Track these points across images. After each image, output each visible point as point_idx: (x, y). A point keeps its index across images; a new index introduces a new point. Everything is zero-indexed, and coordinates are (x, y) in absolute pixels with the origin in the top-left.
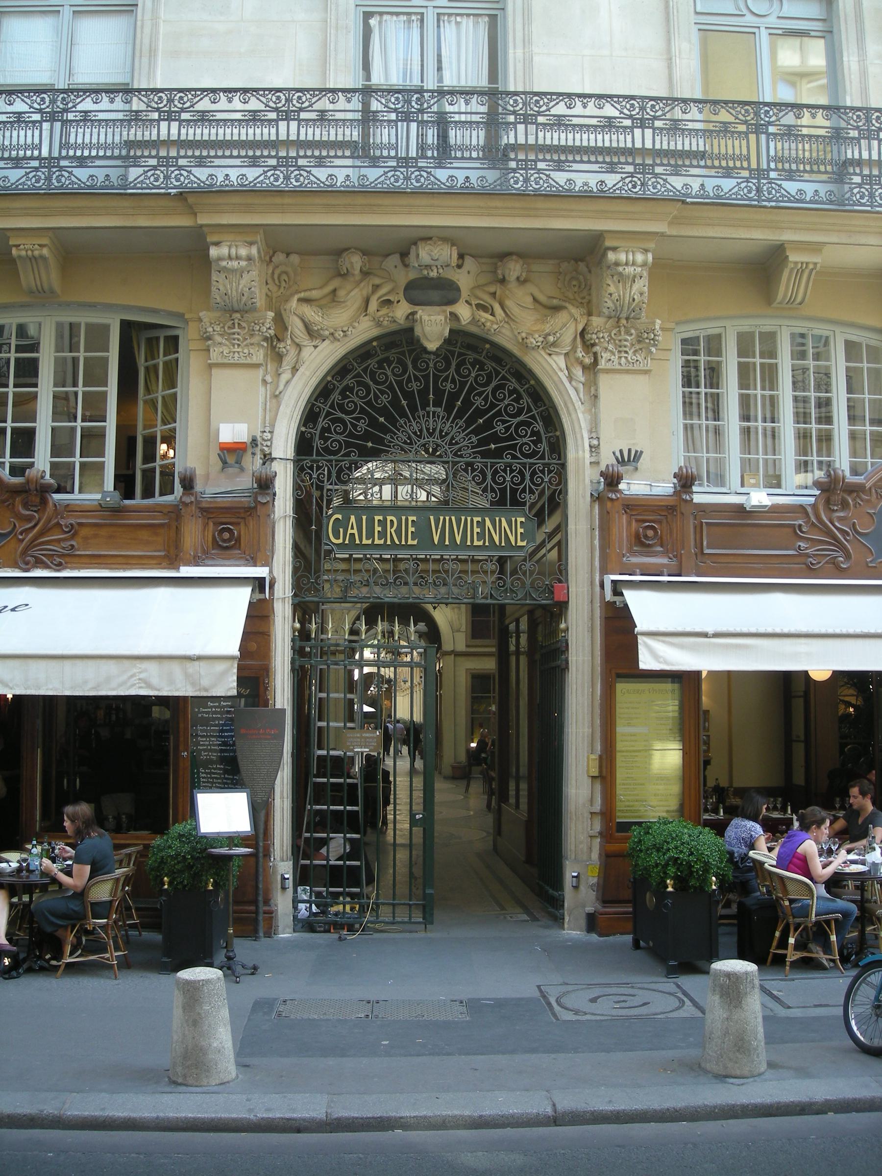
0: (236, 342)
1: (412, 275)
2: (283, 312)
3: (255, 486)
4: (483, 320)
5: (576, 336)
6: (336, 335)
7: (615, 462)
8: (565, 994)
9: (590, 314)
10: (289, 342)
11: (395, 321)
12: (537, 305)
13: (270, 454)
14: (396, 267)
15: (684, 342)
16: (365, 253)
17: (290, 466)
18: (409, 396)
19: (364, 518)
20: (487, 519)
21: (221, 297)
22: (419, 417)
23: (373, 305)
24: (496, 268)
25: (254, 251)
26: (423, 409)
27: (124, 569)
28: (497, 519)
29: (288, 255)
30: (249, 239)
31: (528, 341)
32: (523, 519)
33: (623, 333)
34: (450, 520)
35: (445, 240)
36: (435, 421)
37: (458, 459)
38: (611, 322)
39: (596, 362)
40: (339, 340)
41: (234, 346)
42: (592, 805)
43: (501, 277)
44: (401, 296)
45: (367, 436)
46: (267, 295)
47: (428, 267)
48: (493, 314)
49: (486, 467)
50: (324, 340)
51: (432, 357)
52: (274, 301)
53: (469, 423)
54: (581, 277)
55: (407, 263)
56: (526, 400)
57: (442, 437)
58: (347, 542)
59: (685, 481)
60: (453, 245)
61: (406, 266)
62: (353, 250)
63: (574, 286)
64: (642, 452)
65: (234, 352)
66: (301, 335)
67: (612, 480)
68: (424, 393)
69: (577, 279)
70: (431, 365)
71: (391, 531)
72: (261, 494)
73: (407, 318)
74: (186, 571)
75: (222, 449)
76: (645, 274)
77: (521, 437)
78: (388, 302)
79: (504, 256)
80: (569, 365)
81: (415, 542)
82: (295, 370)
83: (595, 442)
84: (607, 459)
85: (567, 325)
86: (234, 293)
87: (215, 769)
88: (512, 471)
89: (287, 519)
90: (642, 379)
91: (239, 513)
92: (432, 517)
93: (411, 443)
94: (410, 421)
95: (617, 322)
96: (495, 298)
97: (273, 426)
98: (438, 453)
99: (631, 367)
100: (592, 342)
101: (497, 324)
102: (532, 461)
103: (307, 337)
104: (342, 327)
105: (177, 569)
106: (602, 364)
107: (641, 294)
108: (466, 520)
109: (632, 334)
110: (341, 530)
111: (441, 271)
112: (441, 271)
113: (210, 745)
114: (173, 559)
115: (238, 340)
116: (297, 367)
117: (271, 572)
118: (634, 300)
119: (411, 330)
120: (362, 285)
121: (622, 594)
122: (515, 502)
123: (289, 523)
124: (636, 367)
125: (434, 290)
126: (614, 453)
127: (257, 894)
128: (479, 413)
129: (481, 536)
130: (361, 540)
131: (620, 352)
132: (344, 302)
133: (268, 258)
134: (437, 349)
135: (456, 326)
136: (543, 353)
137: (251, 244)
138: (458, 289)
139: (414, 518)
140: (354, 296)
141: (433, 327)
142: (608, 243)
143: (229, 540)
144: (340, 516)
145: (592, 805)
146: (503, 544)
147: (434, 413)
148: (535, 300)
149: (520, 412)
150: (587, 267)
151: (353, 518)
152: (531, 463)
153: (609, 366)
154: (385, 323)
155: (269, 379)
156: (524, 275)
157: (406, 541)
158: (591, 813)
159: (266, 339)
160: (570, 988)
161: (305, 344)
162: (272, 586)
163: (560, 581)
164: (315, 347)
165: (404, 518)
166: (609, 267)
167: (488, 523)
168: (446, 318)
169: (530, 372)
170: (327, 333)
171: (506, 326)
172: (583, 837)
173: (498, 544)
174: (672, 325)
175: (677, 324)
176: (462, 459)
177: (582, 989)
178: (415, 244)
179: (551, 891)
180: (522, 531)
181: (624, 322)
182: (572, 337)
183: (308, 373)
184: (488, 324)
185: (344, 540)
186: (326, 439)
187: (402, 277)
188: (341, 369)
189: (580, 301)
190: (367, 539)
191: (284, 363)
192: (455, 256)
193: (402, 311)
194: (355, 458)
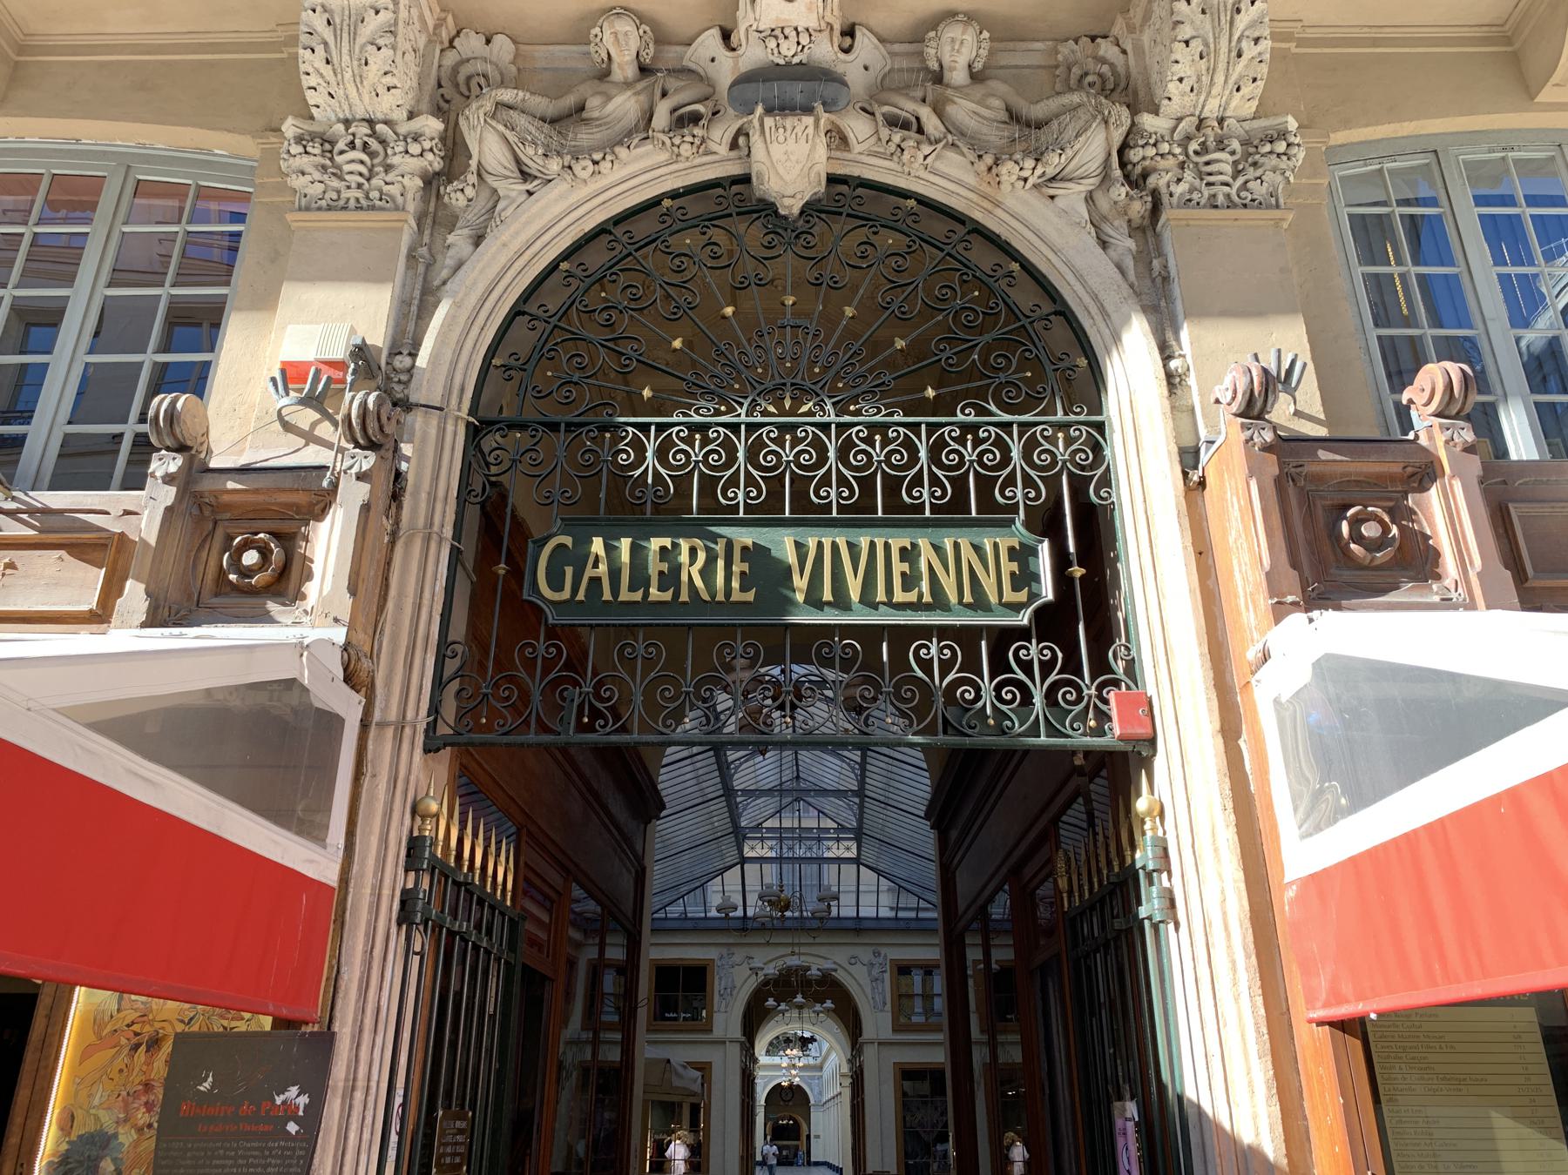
6: (577, 168)
10: (472, 178)
14: (713, 60)
20: (924, 544)
29: (488, 41)
34: (835, 546)
37: (847, 419)
55: (734, 45)
58: (581, 596)
73: (734, 145)
78: (695, 118)
81: (750, 596)
86: (346, 58)
98: (804, 409)
102: (1026, 418)
108: (872, 545)
110: (569, 571)
111: (804, 40)
112: (804, 40)
115: (361, 174)
119: (745, 179)
120: (640, 86)
125: (792, 87)
129: (909, 582)
130: (615, 590)
141: (790, 162)
144: (568, 540)
148: (1008, 110)
151: (597, 546)
152: (1021, 424)
156: (983, 53)
164: (530, 193)
176: (860, 419)
187: (725, 69)
190: (632, 589)
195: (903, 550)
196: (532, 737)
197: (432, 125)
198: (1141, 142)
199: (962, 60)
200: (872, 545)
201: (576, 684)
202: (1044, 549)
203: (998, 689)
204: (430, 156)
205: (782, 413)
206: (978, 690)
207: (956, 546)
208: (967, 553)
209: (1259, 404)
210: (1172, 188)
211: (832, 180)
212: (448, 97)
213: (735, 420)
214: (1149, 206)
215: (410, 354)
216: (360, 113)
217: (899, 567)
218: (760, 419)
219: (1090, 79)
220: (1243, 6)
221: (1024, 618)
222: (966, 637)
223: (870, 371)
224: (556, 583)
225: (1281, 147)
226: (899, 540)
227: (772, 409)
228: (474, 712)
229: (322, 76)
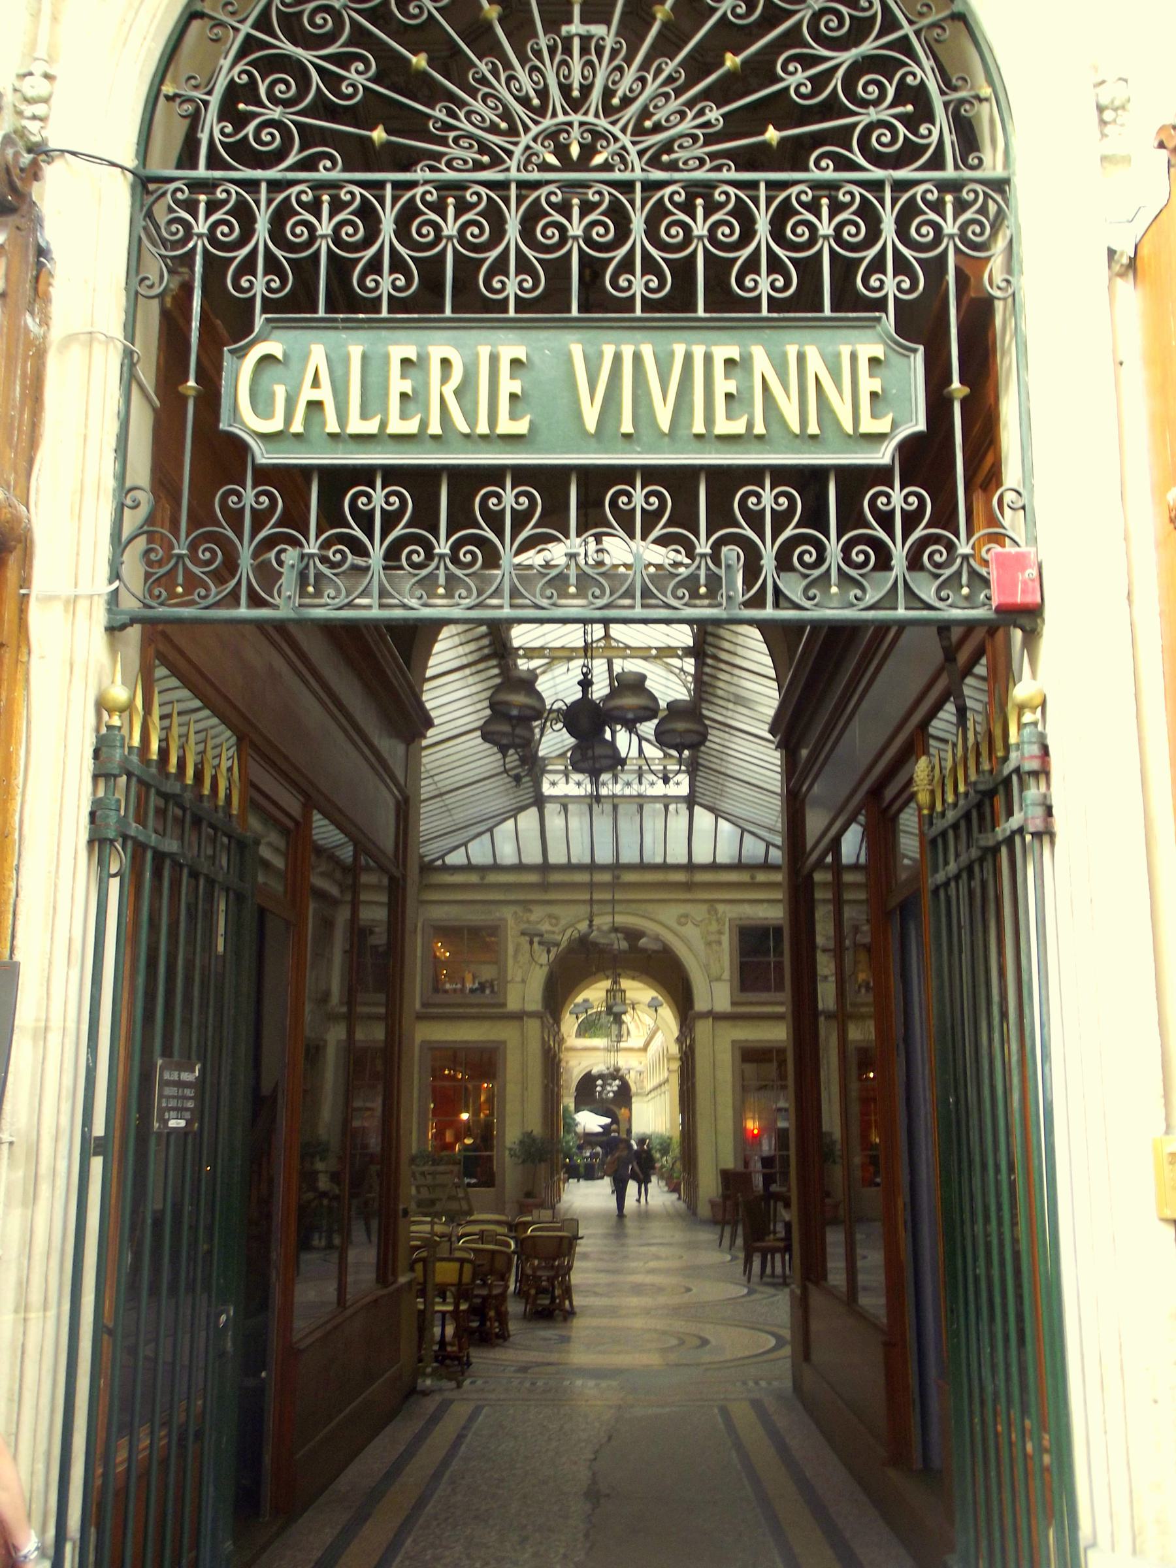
20: (759, 354)
26: (552, 26)
28: (792, 351)
32: (878, 351)
34: (637, 358)
37: (657, 175)
57: (608, 110)
77: (864, 104)
81: (521, 427)
92: (577, 350)
94: (508, 66)
98: (598, 160)
108: (688, 358)
110: (280, 391)
122: (847, 299)
130: (342, 419)
139: (520, 353)
144: (273, 346)
147: (585, 39)
151: (318, 355)
165: (484, 352)
167: (761, 363)
173: (796, 429)
176: (677, 176)
190: (364, 416)
194: (335, 175)
195: (729, 362)
196: (244, 611)
200: (688, 358)
201: (295, 543)
202: (918, 360)
203: (846, 550)
205: (567, 164)
206: (821, 549)
207: (801, 358)
208: (815, 365)
213: (500, 177)
215: (47, 76)
218: (536, 176)
221: (883, 455)
222: (809, 480)
223: (690, 104)
226: (725, 350)
227: (552, 160)
228: (168, 580)
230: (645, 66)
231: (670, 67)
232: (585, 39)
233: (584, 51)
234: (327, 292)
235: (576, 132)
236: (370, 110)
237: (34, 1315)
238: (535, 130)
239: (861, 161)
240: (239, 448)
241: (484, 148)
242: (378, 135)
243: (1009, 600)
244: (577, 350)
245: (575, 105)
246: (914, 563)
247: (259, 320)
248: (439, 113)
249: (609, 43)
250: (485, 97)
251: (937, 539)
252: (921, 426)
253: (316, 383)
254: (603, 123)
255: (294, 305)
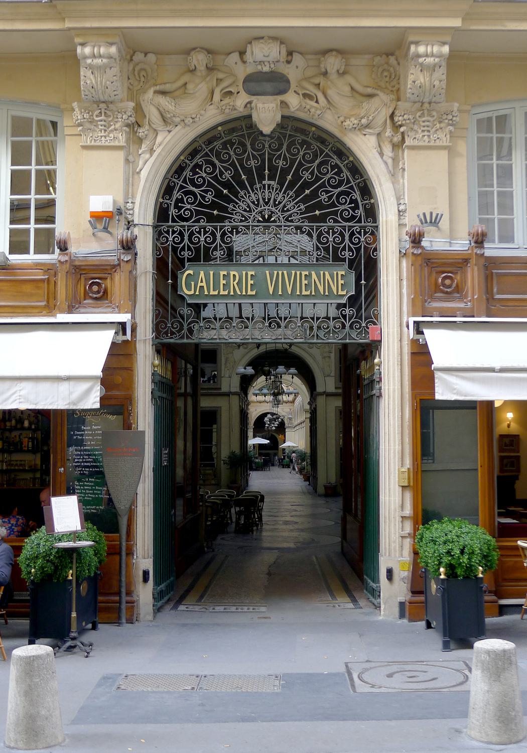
0: (103, 127)
1: (250, 69)
2: (142, 102)
3: (119, 246)
4: (308, 107)
5: (386, 120)
6: (186, 121)
7: (419, 223)
8: (366, 670)
9: (398, 100)
10: (147, 127)
11: (235, 109)
12: (355, 94)
13: (133, 221)
14: (236, 63)
15: (479, 122)
16: (209, 52)
17: (150, 230)
18: (249, 172)
19: (212, 273)
20: (313, 273)
21: (89, 90)
22: (257, 189)
23: (217, 96)
24: (320, 63)
25: (113, 50)
26: (260, 182)
27: (12, 317)
29: (146, 54)
30: (110, 40)
31: (345, 124)
32: (343, 273)
33: (426, 115)
34: (283, 274)
35: (274, 39)
36: (270, 192)
38: (418, 105)
39: (403, 140)
40: (189, 126)
41: (101, 131)
42: (402, 511)
43: (323, 70)
44: (241, 88)
45: (213, 206)
46: (129, 88)
47: (261, 63)
48: (317, 102)
49: (313, 230)
50: (176, 126)
51: (268, 139)
52: (135, 93)
53: (298, 194)
54: (392, 69)
56: (346, 173)
57: (275, 205)
59: (479, 240)
60: (282, 43)
61: (244, 62)
62: (199, 49)
63: (386, 76)
64: (442, 215)
65: (102, 137)
66: (157, 121)
67: (416, 239)
68: (260, 169)
69: (389, 71)
70: (267, 146)
71: (233, 283)
72: (124, 253)
73: (246, 106)
74: (62, 318)
75: (91, 217)
76: (444, 64)
77: (341, 204)
78: (230, 93)
79: (326, 52)
80: (382, 144)
81: (254, 293)
82: (152, 151)
83: (402, 207)
84: (412, 221)
85: (378, 109)
86: (99, 86)
87: (87, 482)
88: (334, 233)
89: (148, 274)
90: (444, 154)
91: (106, 269)
92: (267, 272)
93: (250, 211)
95: (421, 106)
96: (319, 89)
97: (133, 197)
98: (273, 219)
99: (432, 144)
100: (400, 123)
101: (320, 110)
102: (350, 224)
103: (163, 123)
104: (191, 114)
105: (55, 316)
106: (408, 142)
107: (440, 81)
108: (296, 274)
109: (433, 116)
110: (193, 283)
111: (272, 66)
113: (83, 462)
114: (50, 309)
115: (105, 126)
116: (154, 148)
117: (133, 317)
118: (434, 86)
120: (208, 79)
121: (422, 333)
122: (337, 259)
123: (150, 278)
124: (438, 143)
125: (270, 82)
126: (418, 216)
127: (120, 587)
128: (306, 185)
130: (209, 291)
131: (423, 131)
132: (193, 93)
133: (128, 57)
134: (272, 132)
135: (287, 114)
136: (359, 133)
137: (112, 44)
138: (288, 82)
139: (253, 273)
140: (201, 88)
141: (267, 114)
142: (411, 38)
143: (98, 292)
144: (191, 272)
145: (402, 511)
146: (327, 294)
147: (269, 186)
148: (352, 88)
149: (340, 183)
150: (397, 60)
151: (202, 273)
152: (349, 226)
153: (416, 143)
154: (227, 111)
155: (131, 158)
156: (343, 67)
157: (246, 292)
158: (402, 517)
159: (128, 125)
160: (373, 665)
161: (160, 129)
162: (134, 330)
163: (375, 324)
164: (169, 131)
165: (244, 273)
166: (412, 59)
168: (277, 105)
169: (349, 149)
170: (177, 120)
171: (328, 111)
172: (395, 537)
174: (468, 107)
175: (473, 106)
177: (383, 666)
178: (250, 43)
179: (372, 584)
180: (343, 282)
181: (426, 105)
182: (384, 119)
183: (163, 154)
184: (313, 110)
185: (195, 291)
186: (180, 208)
187: (242, 72)
188: (192, 151)
189: (391, 89)
191: (143, 146)
192: (284, 52)
193: (241, 101)
194: (204, 224)
196: (185, 341)
197: (132, 104)
198: (398, 115)
199: (335, 68)
200: (296, 274)
201: (197, 322)
204: (130, 118)
205: (265, 221)
207: (324, 274)
208: (327, 276)
209: (418, 238)
210: (409, 133)
211: (283, 117)
212: (132, 84)
214: (400, 139)
215: (132, 202)
216: (102, 99)
217: (304, 282)
219: (386, 74)
220: (436, 69)
224: (188, 287)
225: (450, 117)
227: (260, 219)
229: (90, 91)
230: (284, 193)
231: (291, 194)
232: (269, 186)
233: (269, 188)
234: (202, 256)
235: (266, 212)
236: (213, 206)
237: (146, 507)
238: (256, 211)
239: (340, 220)
240: (182, 298)
241: (243, 216)
242: (215, 212)
243: (373, 339)
244: (267, 272)
245: (267, 203)
246: (351, 327)
247: (187, 264)
248: (231, 206)
249: (275, 187)
250: (243, 201)
251: (357, 322)
252: (354, 293)
253: (202, 282)
254: (274, 209)
255: (195, 259)
